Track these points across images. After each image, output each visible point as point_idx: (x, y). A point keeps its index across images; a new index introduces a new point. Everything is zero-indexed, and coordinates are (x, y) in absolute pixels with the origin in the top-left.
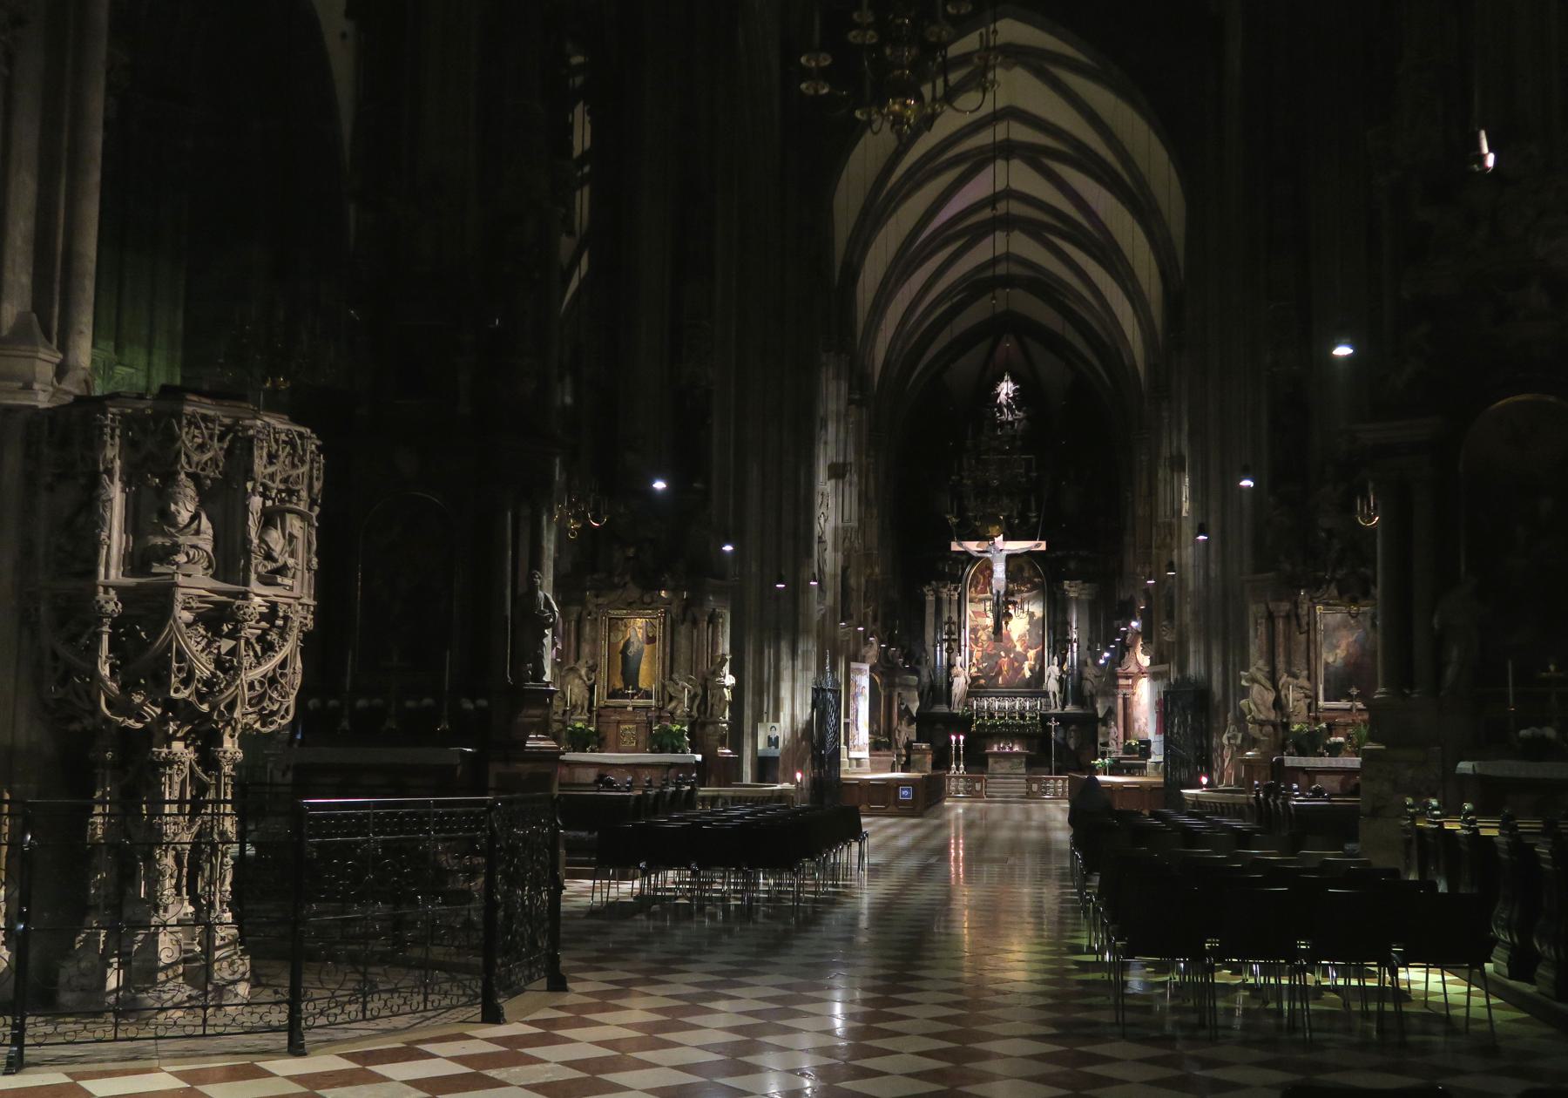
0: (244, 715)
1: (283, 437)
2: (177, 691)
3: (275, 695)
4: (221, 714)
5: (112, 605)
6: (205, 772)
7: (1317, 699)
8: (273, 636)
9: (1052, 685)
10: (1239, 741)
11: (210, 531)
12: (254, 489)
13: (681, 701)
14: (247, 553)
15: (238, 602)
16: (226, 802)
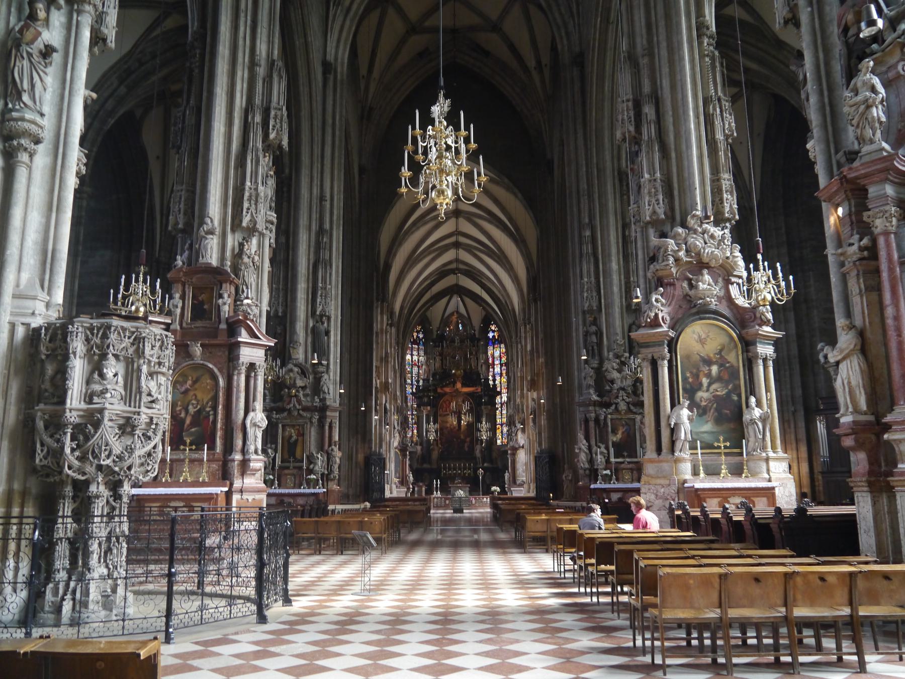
0: (135, 472)
1: (158, 337)
2: (104, 460)
3: (150, 463)
4: (125, 472)
5: (73, 418)
6: (114, 501)
7: (609, 457)
8: (150, 433)
9: (478, 453)
10: (570, 478)
12: (144, 362)
13: (315, 464)
14: (140, 393)
15: (135, 417)
16: (124, 515)
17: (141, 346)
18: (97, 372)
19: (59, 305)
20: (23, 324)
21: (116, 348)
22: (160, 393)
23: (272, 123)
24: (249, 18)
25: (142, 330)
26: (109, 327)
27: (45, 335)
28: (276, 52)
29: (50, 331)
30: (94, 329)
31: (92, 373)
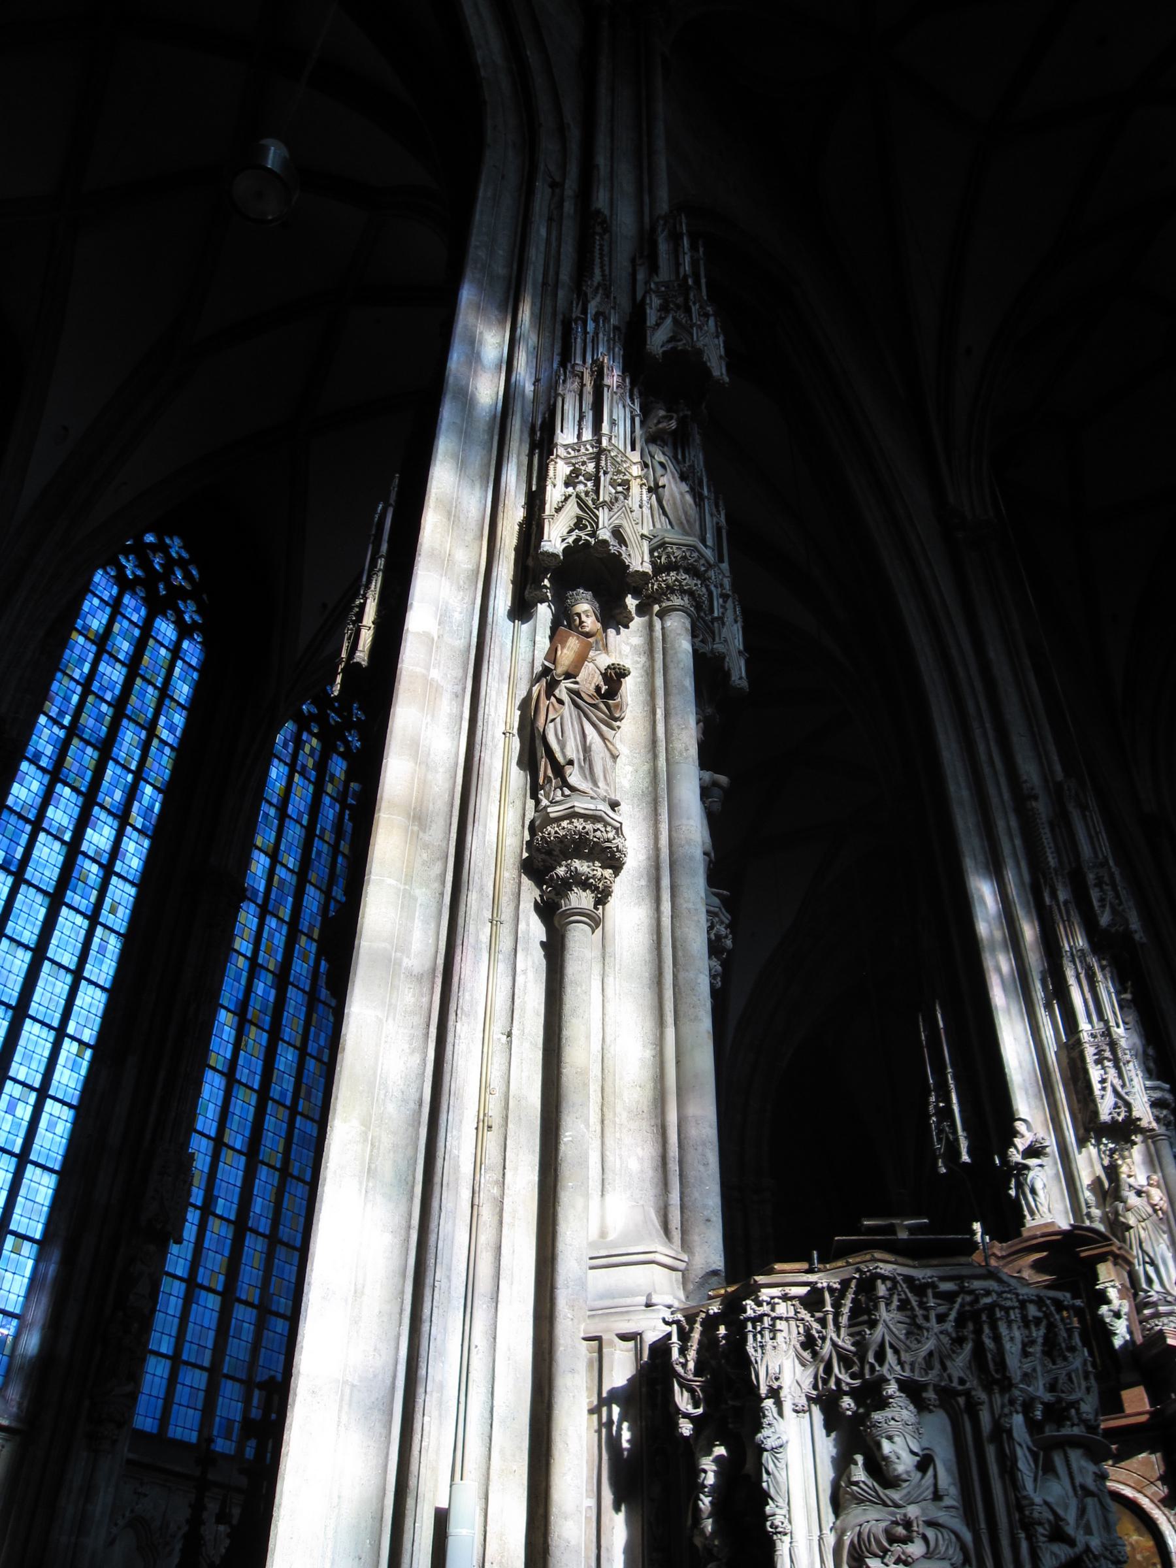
11: (953, 1491)
17: (989, 1343)
18: (859, 1459)
19: (715, 1273)
20: (624, 1337)
21: (905, 1356)
22: (1088, 1531)
23: (1095, 895)
24: (988, 725)
25: (977, 1284)
26: (867, 1285)
27: (683, 1351)
28: (1058, 768)
29: (696, 1335)
30: (822, 1303)
31: (842, 1464)
